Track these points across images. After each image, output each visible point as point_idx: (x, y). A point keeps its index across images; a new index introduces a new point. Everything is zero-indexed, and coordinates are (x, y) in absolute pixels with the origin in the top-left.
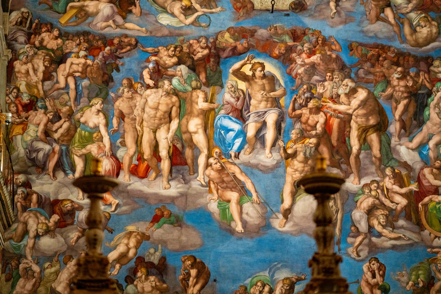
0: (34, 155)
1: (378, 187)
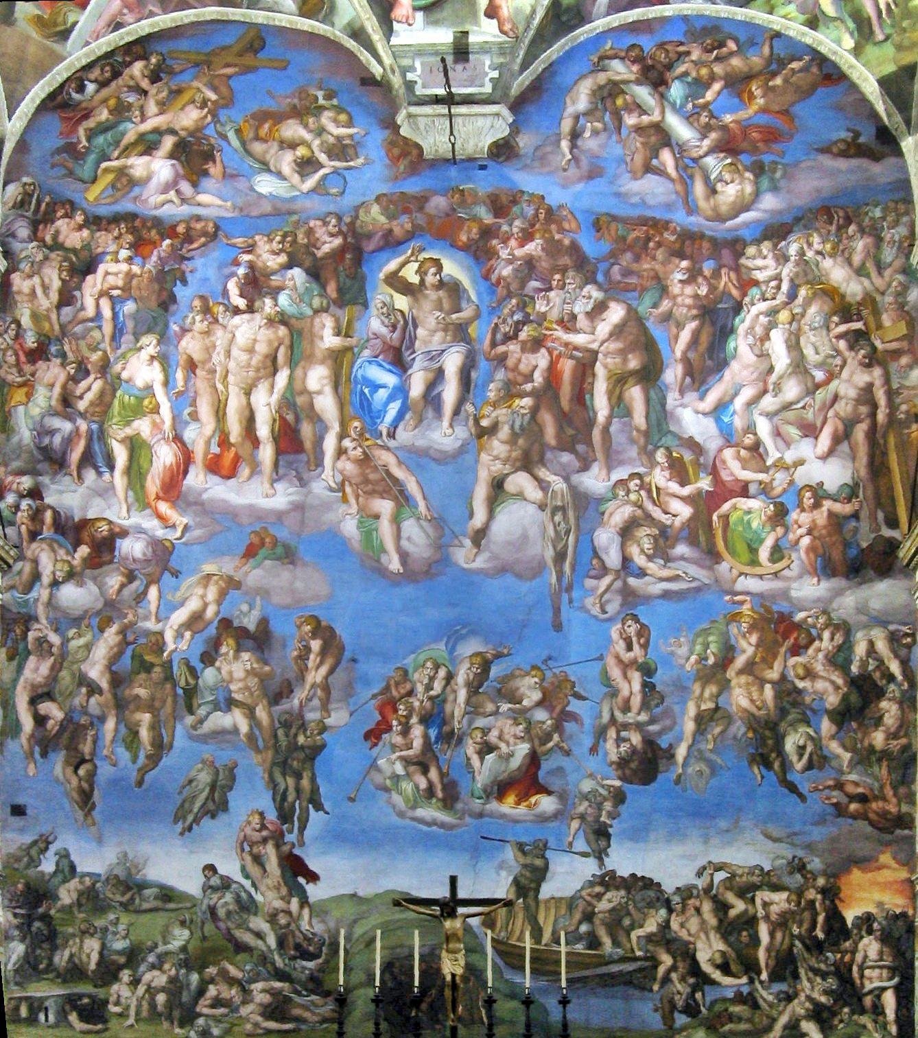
0: (46, 441)
1: (642, 487)
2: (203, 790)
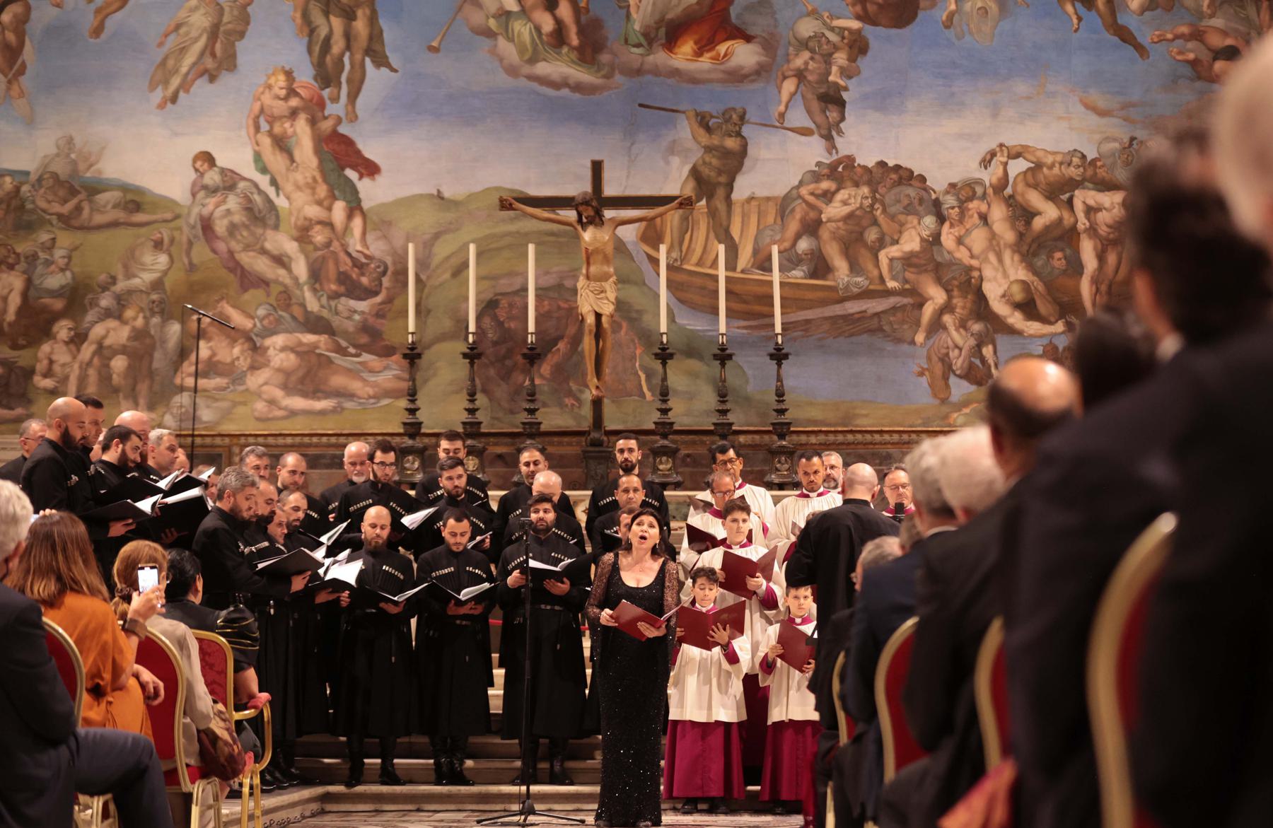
2: (196, 40)
